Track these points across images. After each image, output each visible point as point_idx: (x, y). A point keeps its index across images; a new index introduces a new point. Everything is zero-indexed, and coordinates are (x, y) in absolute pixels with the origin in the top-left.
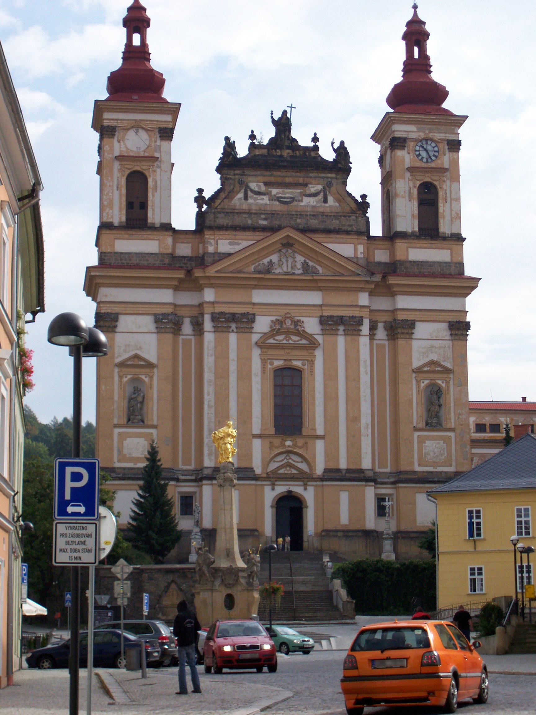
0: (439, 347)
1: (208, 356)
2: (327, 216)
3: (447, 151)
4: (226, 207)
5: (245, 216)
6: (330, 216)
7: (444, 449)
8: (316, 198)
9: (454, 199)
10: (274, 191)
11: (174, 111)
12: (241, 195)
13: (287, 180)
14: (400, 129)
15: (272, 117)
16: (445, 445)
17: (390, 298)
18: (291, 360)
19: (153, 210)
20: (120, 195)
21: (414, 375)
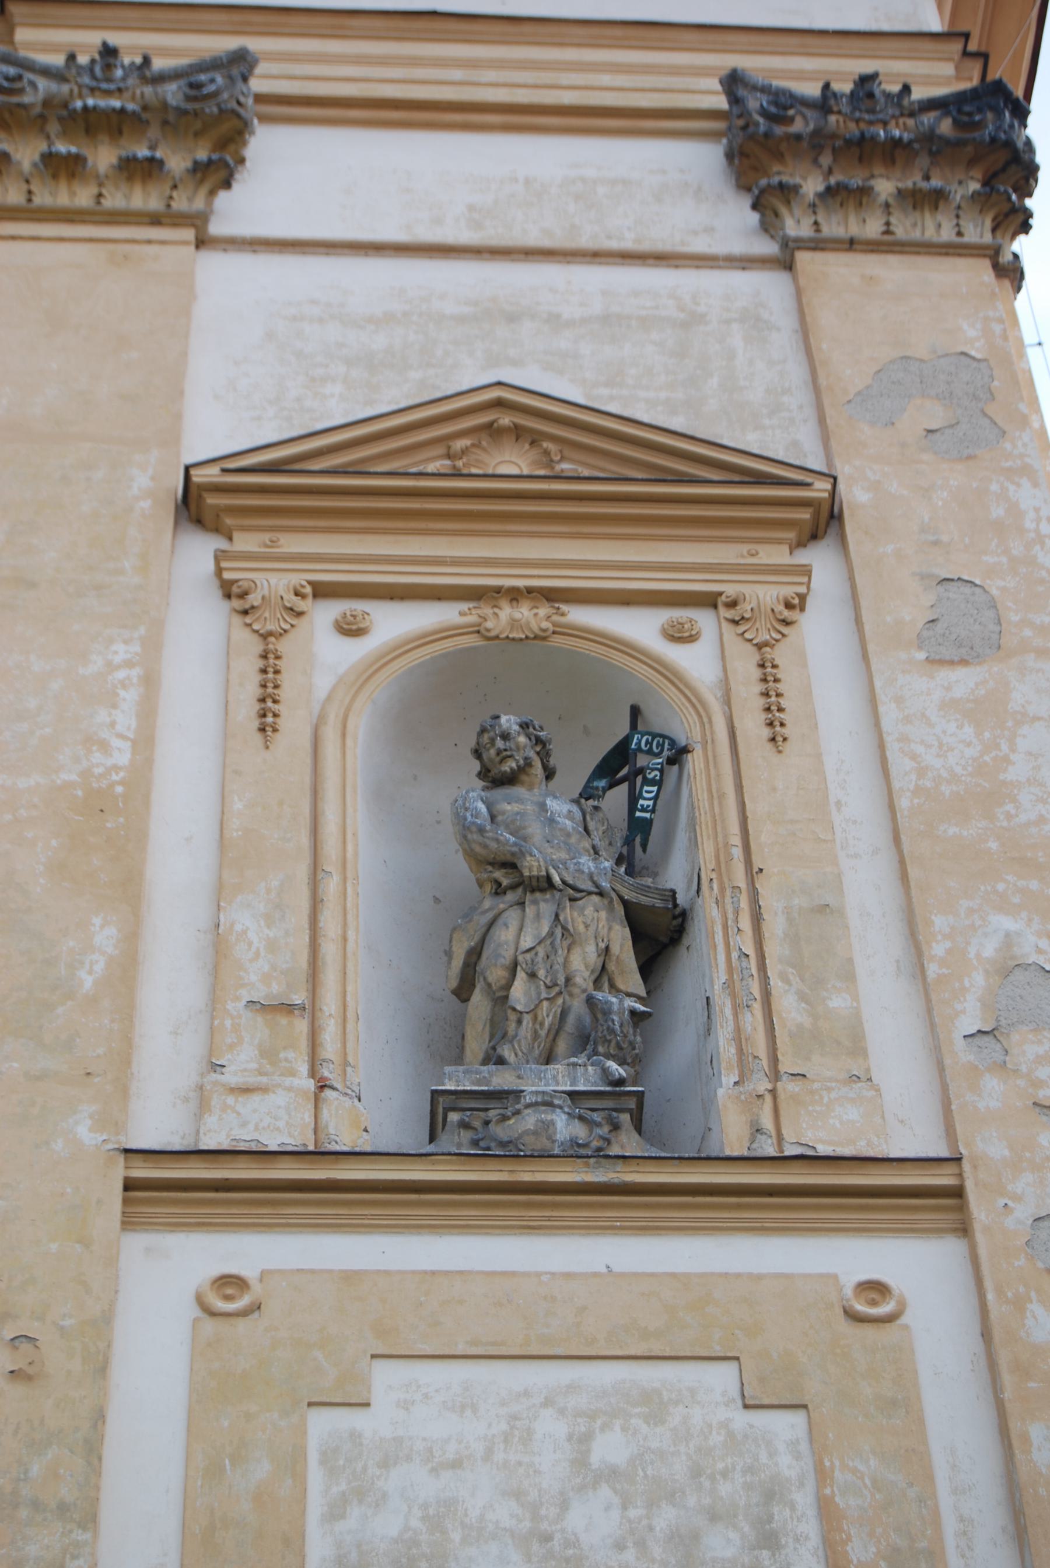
0: (606, 319)
7: (772, 1493)
16: (788, 1426)
21: (199, 552)
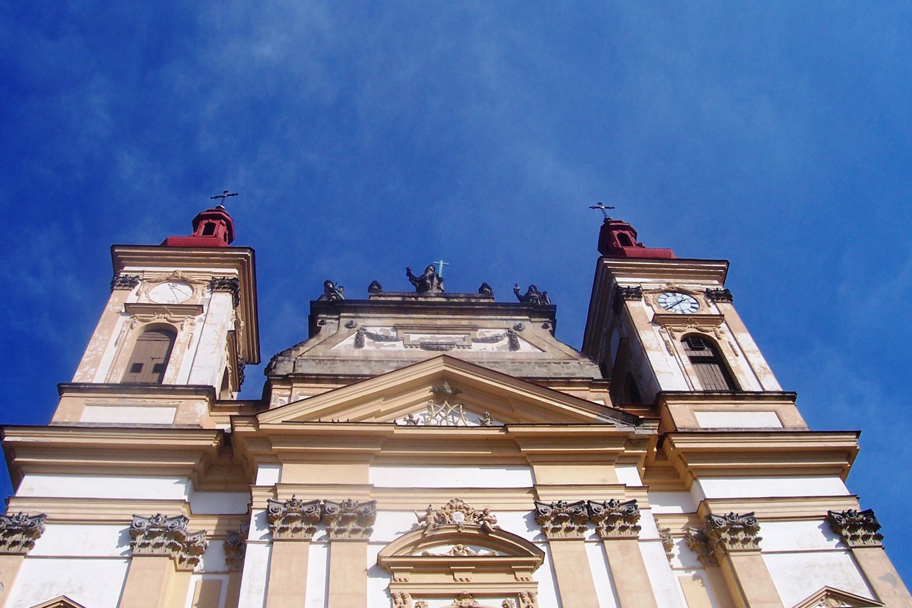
1: (250, 592)
2: (522, 363)
3: (711, 304)
4: (321, 354)
5: (357, 364)
6: (529, 363)
8: (495, 344)
9: (748, 351)
10: (414, 337)
11: (242, 262)
12: (351, 340)
13: (439, 322)
14: (623, 281)
15: (409, 274)
17: (684, 494)
18: (473, 596)
19: (178, 370)
20: (119, 353)
